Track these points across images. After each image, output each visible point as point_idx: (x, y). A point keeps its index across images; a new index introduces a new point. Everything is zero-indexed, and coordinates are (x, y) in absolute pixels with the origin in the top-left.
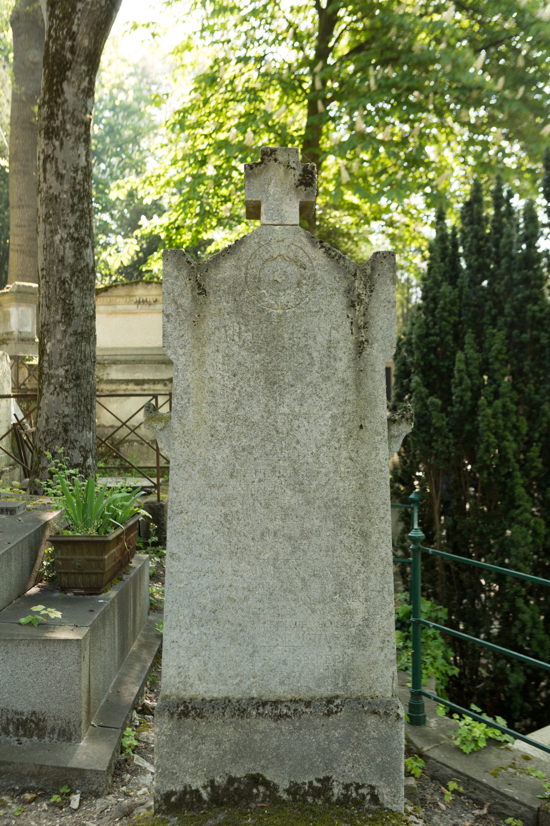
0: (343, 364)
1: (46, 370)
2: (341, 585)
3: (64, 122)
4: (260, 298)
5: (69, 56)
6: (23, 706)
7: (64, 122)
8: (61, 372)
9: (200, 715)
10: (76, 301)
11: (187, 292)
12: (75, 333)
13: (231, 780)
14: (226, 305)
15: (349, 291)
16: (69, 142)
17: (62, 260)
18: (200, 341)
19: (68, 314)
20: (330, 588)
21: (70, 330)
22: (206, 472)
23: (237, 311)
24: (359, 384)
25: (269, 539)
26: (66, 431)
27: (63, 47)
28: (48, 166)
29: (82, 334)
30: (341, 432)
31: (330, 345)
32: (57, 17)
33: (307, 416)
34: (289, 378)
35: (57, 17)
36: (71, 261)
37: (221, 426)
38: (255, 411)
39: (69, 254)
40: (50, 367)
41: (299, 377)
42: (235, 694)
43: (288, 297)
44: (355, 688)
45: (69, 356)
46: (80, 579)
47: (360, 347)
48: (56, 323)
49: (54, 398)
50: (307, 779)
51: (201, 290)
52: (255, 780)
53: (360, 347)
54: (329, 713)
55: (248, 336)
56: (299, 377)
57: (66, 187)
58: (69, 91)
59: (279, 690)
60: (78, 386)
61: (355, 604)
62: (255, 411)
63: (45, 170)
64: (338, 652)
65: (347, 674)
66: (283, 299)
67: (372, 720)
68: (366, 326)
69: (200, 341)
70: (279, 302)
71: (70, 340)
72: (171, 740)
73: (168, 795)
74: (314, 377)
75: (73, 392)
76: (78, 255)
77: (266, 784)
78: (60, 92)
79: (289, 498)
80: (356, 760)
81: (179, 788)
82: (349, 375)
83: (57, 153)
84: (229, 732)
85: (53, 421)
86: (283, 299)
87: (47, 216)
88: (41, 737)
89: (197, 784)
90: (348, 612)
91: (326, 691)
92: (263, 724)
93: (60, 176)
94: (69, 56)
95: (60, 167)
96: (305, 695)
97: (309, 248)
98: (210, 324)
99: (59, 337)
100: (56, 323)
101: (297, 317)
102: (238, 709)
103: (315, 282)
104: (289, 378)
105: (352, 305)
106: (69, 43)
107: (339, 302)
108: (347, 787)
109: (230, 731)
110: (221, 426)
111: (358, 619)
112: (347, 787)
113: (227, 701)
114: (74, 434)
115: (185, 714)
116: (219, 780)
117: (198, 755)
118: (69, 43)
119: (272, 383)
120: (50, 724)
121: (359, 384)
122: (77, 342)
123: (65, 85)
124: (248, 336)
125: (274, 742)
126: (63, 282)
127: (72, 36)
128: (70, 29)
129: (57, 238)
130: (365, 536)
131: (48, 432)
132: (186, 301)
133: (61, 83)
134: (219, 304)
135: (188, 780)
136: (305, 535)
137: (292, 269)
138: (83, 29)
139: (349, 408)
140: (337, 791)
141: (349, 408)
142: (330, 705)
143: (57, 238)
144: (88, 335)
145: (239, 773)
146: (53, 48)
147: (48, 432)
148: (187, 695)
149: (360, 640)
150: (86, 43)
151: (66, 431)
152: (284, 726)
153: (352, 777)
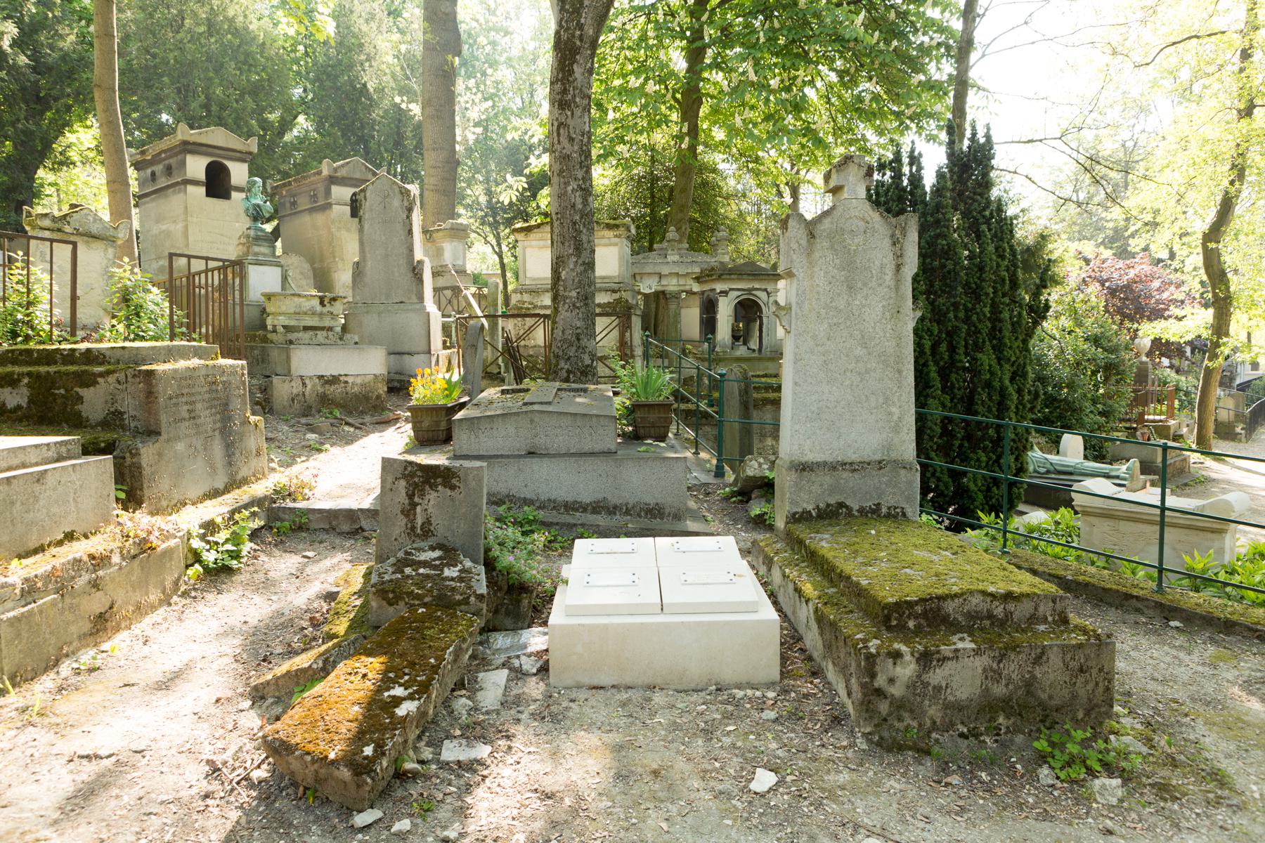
0: (889, 277)
1: (561, 293)
2: (887, 399)
3: (574, 96)
4: (844, 240)
5: (578, 43)
6: (651, 501)
7: (574, 96)
8: (574, 294)
9: (812, 470)
10: (584, 238)
11: (804, 236)
12: (584, 263)
13: (828, 505)
14: (826, 244)
15: (892, 236)
16: (578, 112)
17: (573, 206)
18: (811, 264)
19: (578, 249)
20: (881, 400)
21: (580, 261)
22: (814, 337)
23: (832, 247)
24: (897, 288)
25: (848, 374)
26: (578, 340)
27: (573, 36)
28: (562, 131)
29: (588, 264)
30: (888, 315)
31: (882, 267)
32: (567, 11)
33: (869, 306)
34: (860, 285)
35: (567, 11)
36: (580, 206)
37: (823, 312)
38: (841, 303)
39: (579, 201)
40: (565, 290)
41: (865, 284)
42: (829, 459)
43: (859, 239)
44: (894, 455)
45: (580, 282)
46: (652, 431)
47: (898, 267)
48: (569, 256)
49: (568, 314)
50: (869, 504)
51: (812, 235)
52: (841, 505)
53: (898, 267)
54: (881, 468)
55: (837, 261)
56: (865, 284)
57: (576, 148)
58: (578, 70)
59: (853, 457)
60: (586, 305)
61: (894, 410)
62: (841, 303)
63: (559, 135)
64: (884, 436)
65: (889, 447)
66: (856, 241)
67: (903, 472)
68: (901, 256)
69: (811, 264)
70: (854, 243)
71: (580, 269)
72: (796, 484)
73: (795, 514)
74: (873, 284)
75: (583, 310)
76: (585, 202)
77: (847, 507)
78: (571, 72)
79: (859, 351)
80: (894, 494)
81: (800, 510)
82: (892, 283)
83: (569, 121)
84: (827, 479)
85: (568, 332)
86: (856, 241)
87: (561, 171)
88: (662, 518)
89: (810, 507)
90: (890, 414)
91: (878, 457)
92: (846, 475)
93: (571, 140)
94: (578, 43)
95: (572, 131)
96: (867, 460)
97: (871, 212)
98: (817, 255)
99: (572, 266)
100: (569, 256)
101: (864, 250)
102: (833, 467)
103: (874, 231)
104: (860, 285)
105: (894, 244)
106: (578, 33)
107: (887, 242)
108: (889, 508)
109: (827, 478)
110: (823, 312)
111: (895, 418)
112: (889, 508)
113: (825, 463)
114: (584, 342)
115: (804, 469)
116: (822, 505)
117: (810, 492)
118: (578, 33)
119: (850, 288)
120: (667, 511)
121: (897, 288)
122: (585, 271)
123: (575, 66)
124: (837, 261)
125: (851, 484)
126: (575, 223)
127: (581, 27)
128: (579, 21)
129: (570, 188)
130: (900, 372)
131: (564, 341)
132: (804, 242)
133: (572, 65)
134: (822, 244)
135: (805, 505)
136: (867, 372)
137: (862, 224)
138: (589, 21)
139: (892, 301)
140: (884, 510)
141: (892, 301)
142: (880, 465)
143: (570, 188)
144: (590, 265)
145: (832, 501)
146: (564, 36)
147: (564, 341)
148: (803, 460)
149: (896, 429)
150: (591, 32)
151: (578, 340)
152: (856, 475)
153: (892, 503)
